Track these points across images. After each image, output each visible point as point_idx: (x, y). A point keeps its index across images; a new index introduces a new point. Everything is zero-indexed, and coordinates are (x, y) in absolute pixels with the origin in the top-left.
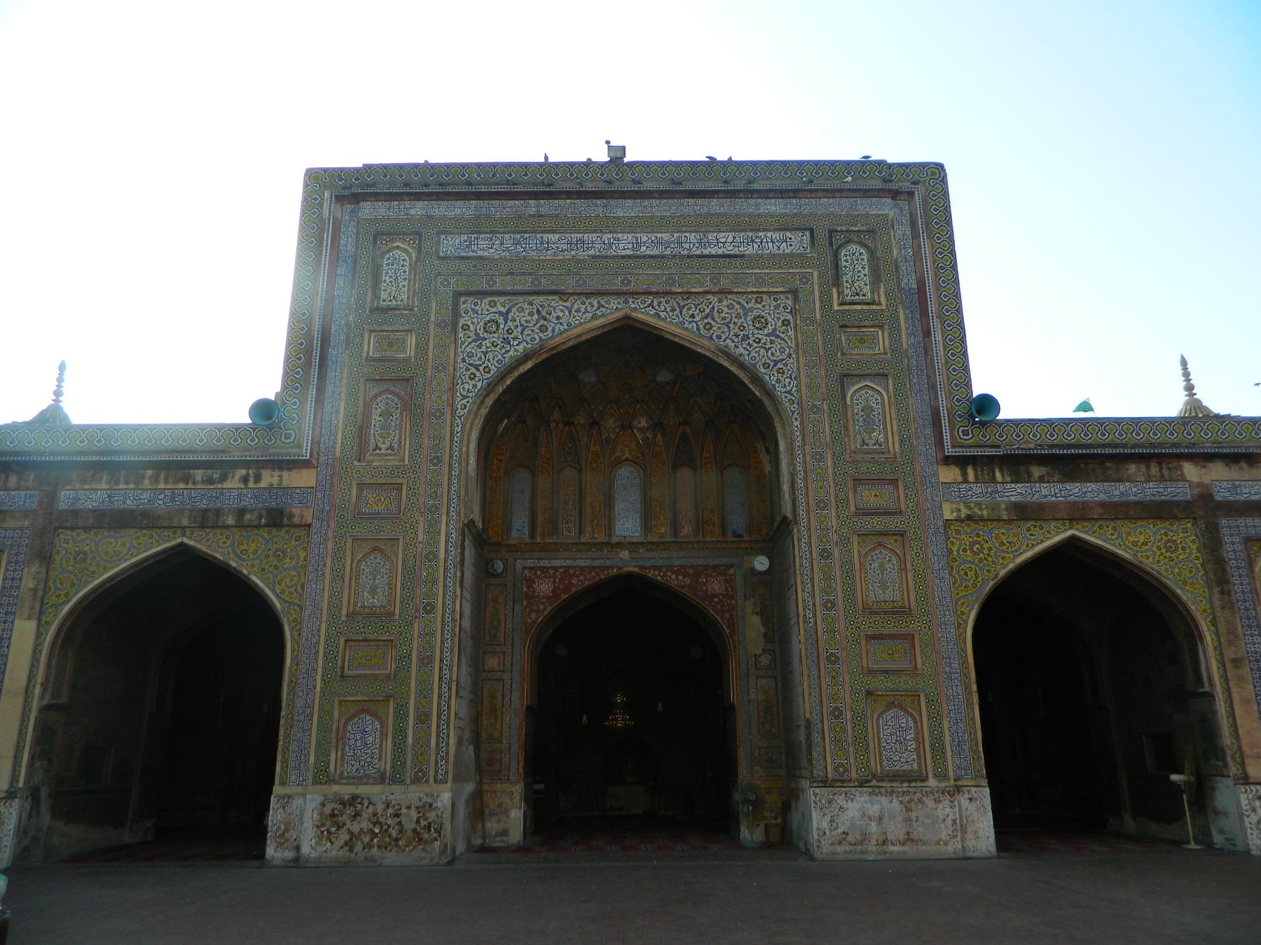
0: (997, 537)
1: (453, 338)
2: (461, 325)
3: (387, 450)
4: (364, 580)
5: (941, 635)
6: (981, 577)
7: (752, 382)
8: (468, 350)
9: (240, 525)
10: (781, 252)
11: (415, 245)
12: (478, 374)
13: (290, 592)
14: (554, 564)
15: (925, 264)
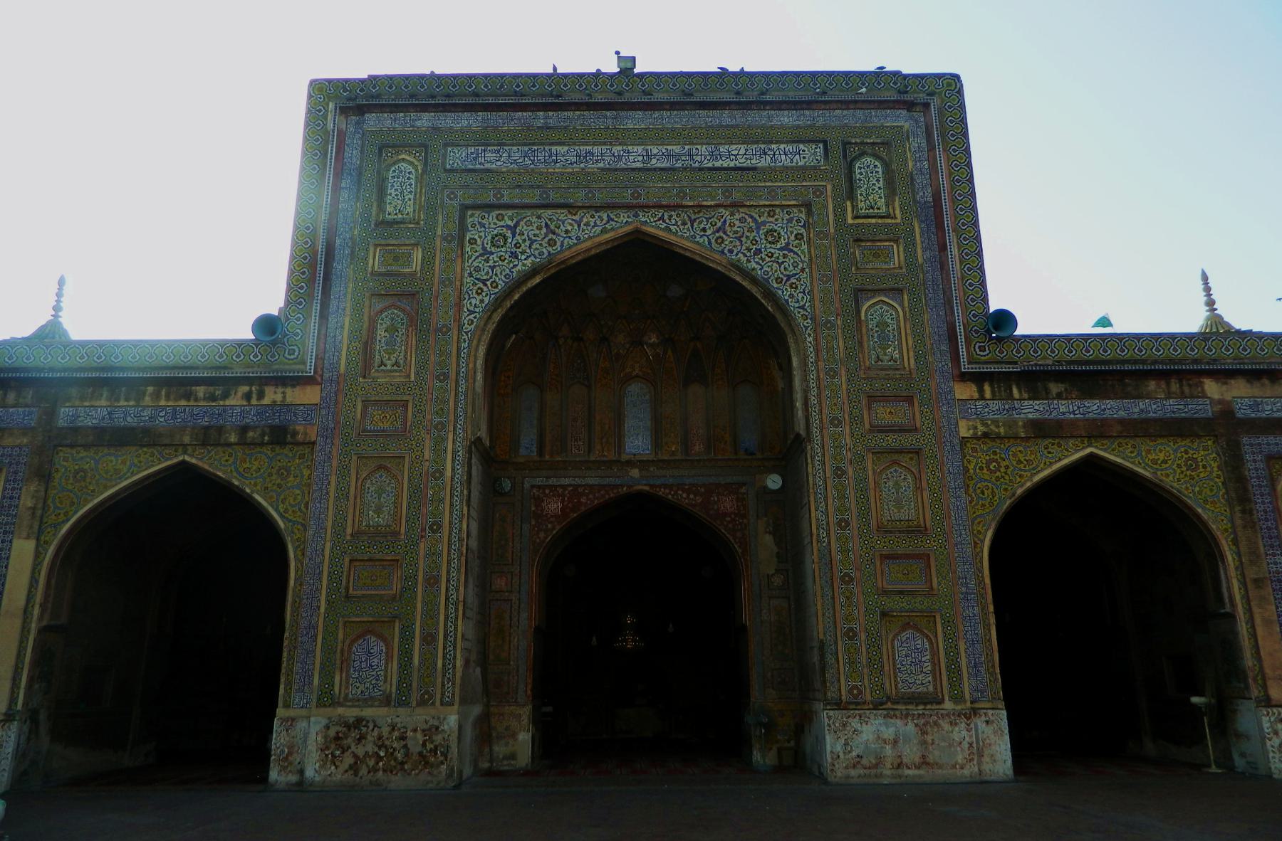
0: (1015, 455)
1: (459, 252)
2: (468, 239)
3: (393, 366)
4: (370, 498)
5: (956, 555)
6: (997, 496)
7: (765, 297)
8: (475, 264)
9: (243, 443)
10: (794, 164)
11: (421, 158)
12: (485, 289)
13: (293, 511)
14: (563, 483)
15: (940, 177)
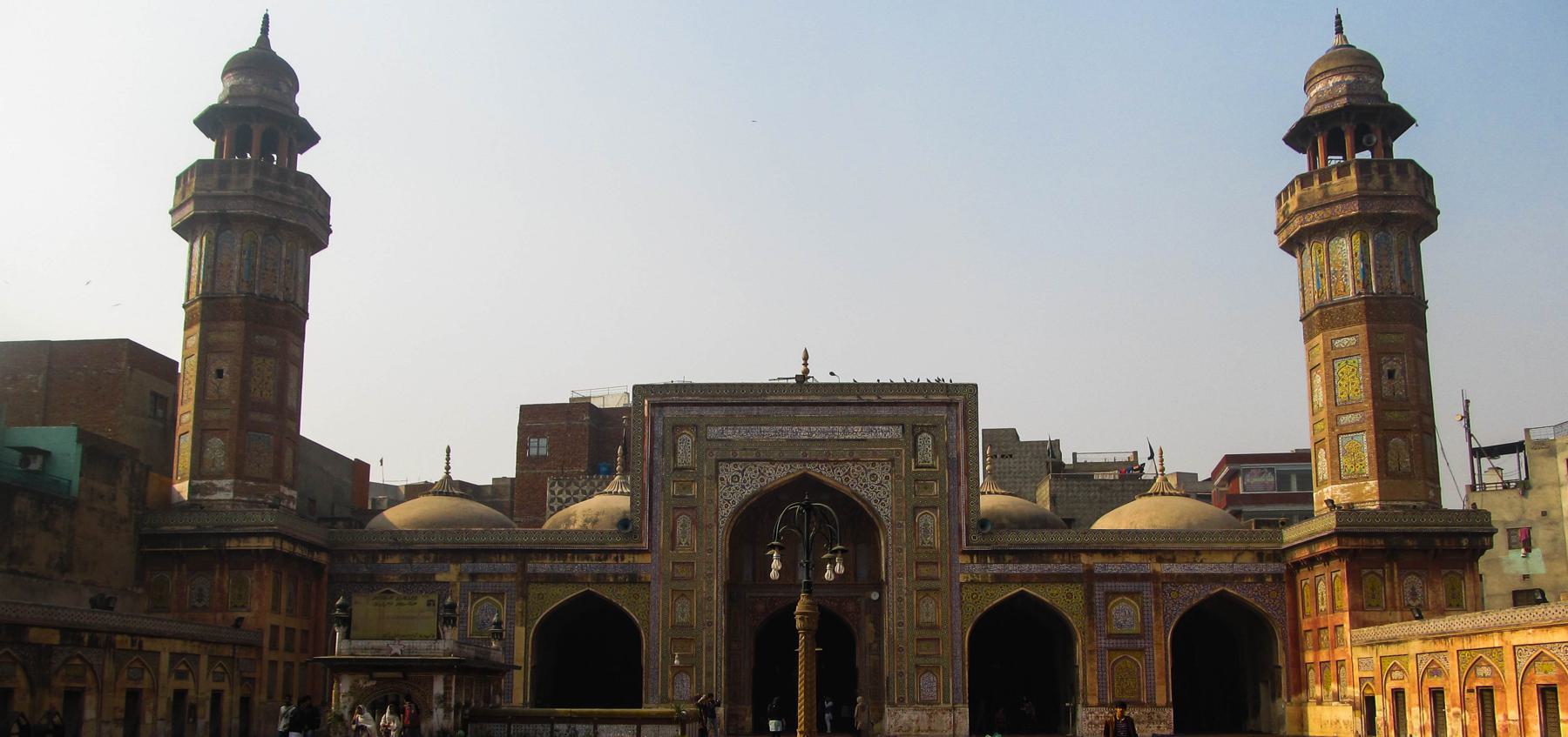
9: (616, 582)
